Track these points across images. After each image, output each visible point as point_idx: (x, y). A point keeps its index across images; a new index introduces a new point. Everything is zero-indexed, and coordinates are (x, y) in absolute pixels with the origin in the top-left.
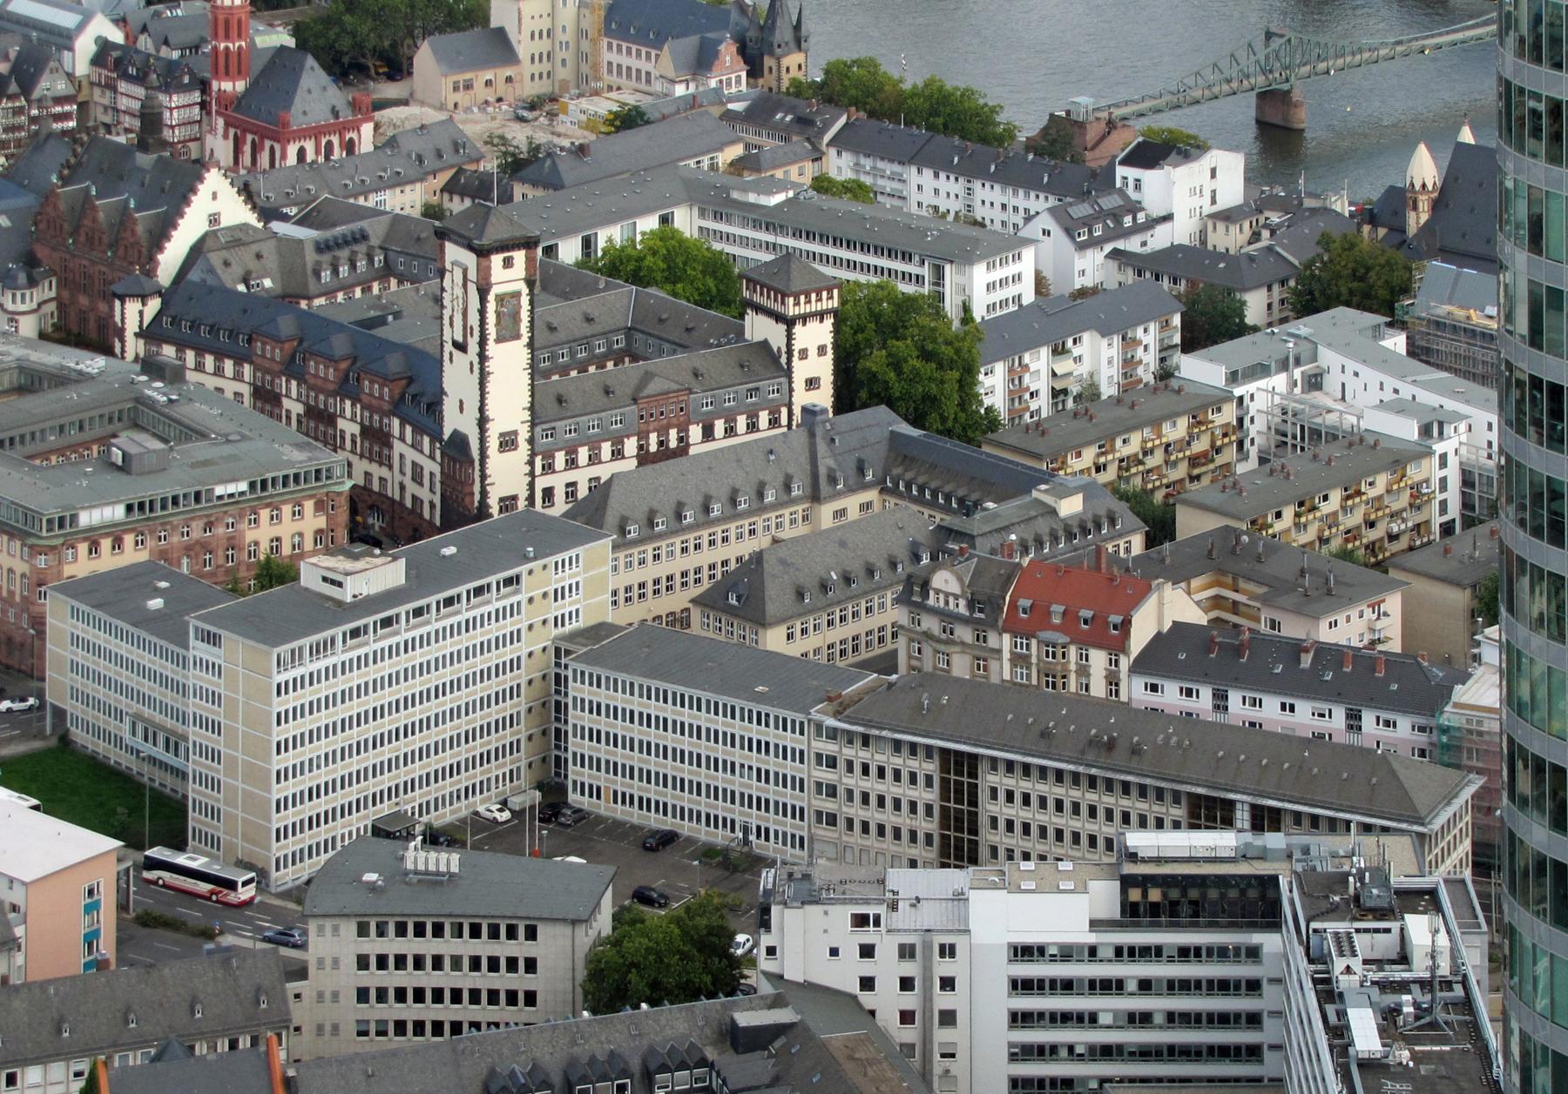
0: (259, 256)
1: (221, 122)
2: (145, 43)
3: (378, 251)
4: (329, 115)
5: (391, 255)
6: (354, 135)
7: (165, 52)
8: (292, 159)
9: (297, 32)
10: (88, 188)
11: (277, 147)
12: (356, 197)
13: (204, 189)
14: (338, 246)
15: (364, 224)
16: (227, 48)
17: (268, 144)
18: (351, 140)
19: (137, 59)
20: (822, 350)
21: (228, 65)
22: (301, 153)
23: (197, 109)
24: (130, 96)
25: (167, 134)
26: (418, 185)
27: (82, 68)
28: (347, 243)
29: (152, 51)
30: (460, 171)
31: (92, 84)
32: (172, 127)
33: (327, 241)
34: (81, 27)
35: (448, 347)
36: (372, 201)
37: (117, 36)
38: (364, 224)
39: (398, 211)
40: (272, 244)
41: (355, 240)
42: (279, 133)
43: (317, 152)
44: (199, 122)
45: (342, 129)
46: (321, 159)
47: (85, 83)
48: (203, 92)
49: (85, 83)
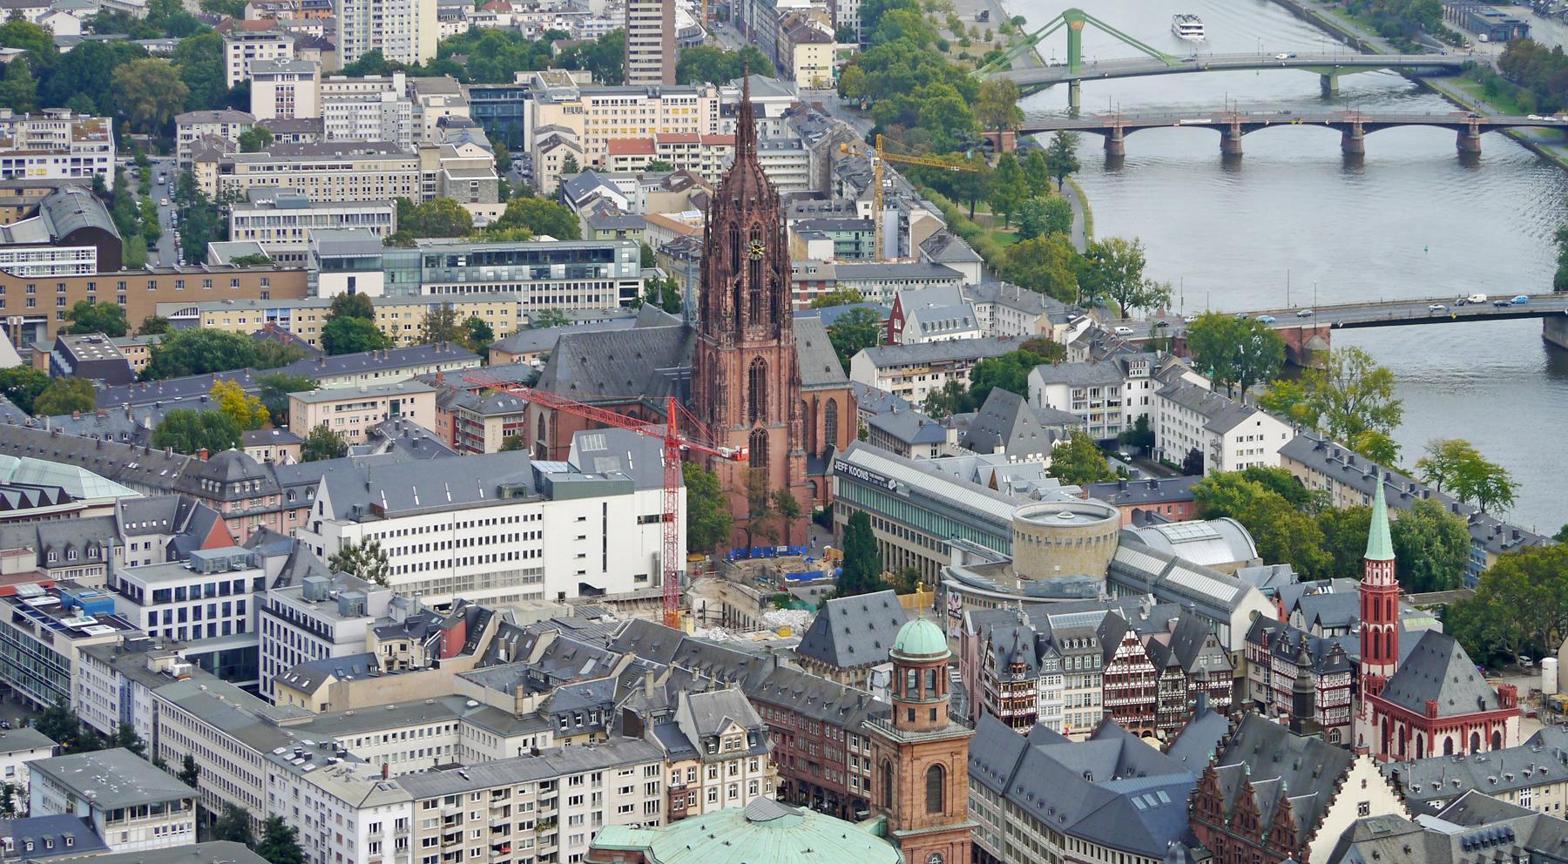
0: (1407, 850)
1: (1370, 707)
2: (1298, 621)
3: (1523, 853)
4: (1477, 708)
5: (1537, 858)
6: (1499, 728)
8: (1439, 750)
9: (1443, 615)
10: (1242, 769)
11: (1425, 736)
12: (1503, 792)
14: (1485, 845)
15: (1509, 823)
16: (1376, 630)
17: (1415, 732)
18: (1497, 732)
19: (1291, 636)
21: (1379, 647)
22: (1449, 744)
23: (1347, 692)
24: (1283, 676)
25: (1318, 716)
26: (1563, 785)
27: (1237, 644)
28: (1493, 842)
31: (1247, 660)
32: (1324, 710)
33: (1473, 838)
34: (1238, 599)
36: (1516, 800)
37: (1271, 612)
38: (1509, 823)
39: (1542, 811)
40: (1419, 838)
41: (1502, 840)
42: (1429, 723)
43: (1464, 745)
44: (1349, 705)
45: (1487, 722)
46: (1467, 752)
47: (1240, 659)
48: (1354, 675)
49: (1240, 659)
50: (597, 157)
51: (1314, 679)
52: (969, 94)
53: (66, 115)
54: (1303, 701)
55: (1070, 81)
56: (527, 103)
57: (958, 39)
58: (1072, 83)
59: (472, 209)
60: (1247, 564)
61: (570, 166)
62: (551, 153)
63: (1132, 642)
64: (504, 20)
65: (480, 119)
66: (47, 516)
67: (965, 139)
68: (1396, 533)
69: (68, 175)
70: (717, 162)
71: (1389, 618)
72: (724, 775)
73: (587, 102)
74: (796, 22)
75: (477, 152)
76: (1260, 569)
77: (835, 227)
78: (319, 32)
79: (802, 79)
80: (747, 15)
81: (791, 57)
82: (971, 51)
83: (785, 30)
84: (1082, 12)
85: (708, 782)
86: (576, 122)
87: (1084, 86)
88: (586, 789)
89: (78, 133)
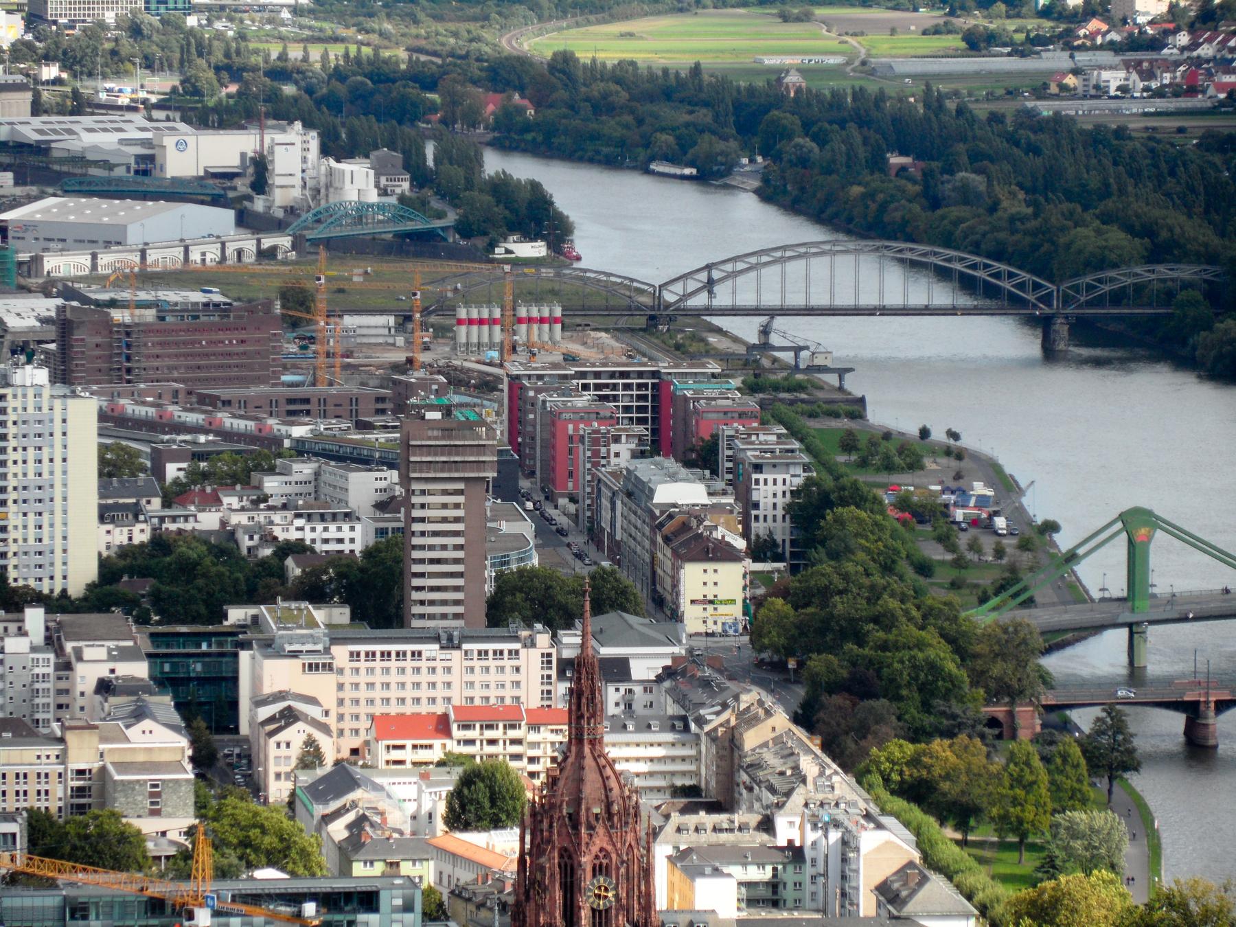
50: (356, 742)
52: (958, 643)
55: (1130, 626)
56: (244, 656)
57: (949, 557)
58: (1134, 630)
59: (148, 826)
61: (311, 757)
62: (282, 736)
64: (208, 521)
65: (162, 682)
67: (954, 717)
73: (341, 653)
74: (685, 527)
77: (741, 856)
79: (693, 619)
80: (606, 515)
81: (676, 584)
82: (972, 577)
83: (667, 540)
84: (1149, 513)
87: (1153, 631)
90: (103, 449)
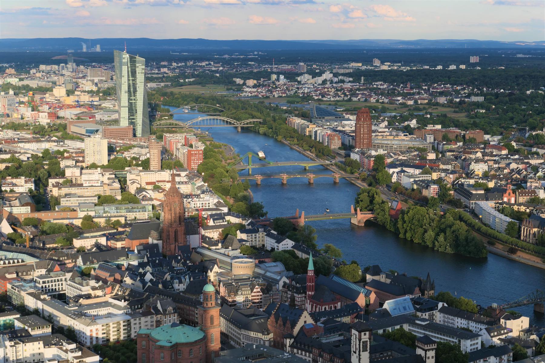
1: (309, 301)
7: (298, 285)
8: (323, 310)
11: (320, 307)
13: (303, 315)
17: (318, 306)
20: (432, 357)
22: (325, 308)
23: (304, 298)
27: (281, 288)
29: (295, 285)
30: (358, 314)
34: (281, 279)
35: (352, 352)
37: (288, 281)
48: (305, 294)
51: (295, 295)
53: (24, 178)
54: (293, 299)
60: (283, 271)
63: (257, 288)
66: (18, 266)
68: (315, 263)
69: (24, 191)
70: (168, 186)
71: (313, 282)
72: (168, 317)
73: (141, 173)
75: (117, 185)
76: (286, 272)
78: (81, 159)
85: (164, 319)
86: (138, 178)
88: (137, 321)
89: (26, 182)
90: (108, 146)
